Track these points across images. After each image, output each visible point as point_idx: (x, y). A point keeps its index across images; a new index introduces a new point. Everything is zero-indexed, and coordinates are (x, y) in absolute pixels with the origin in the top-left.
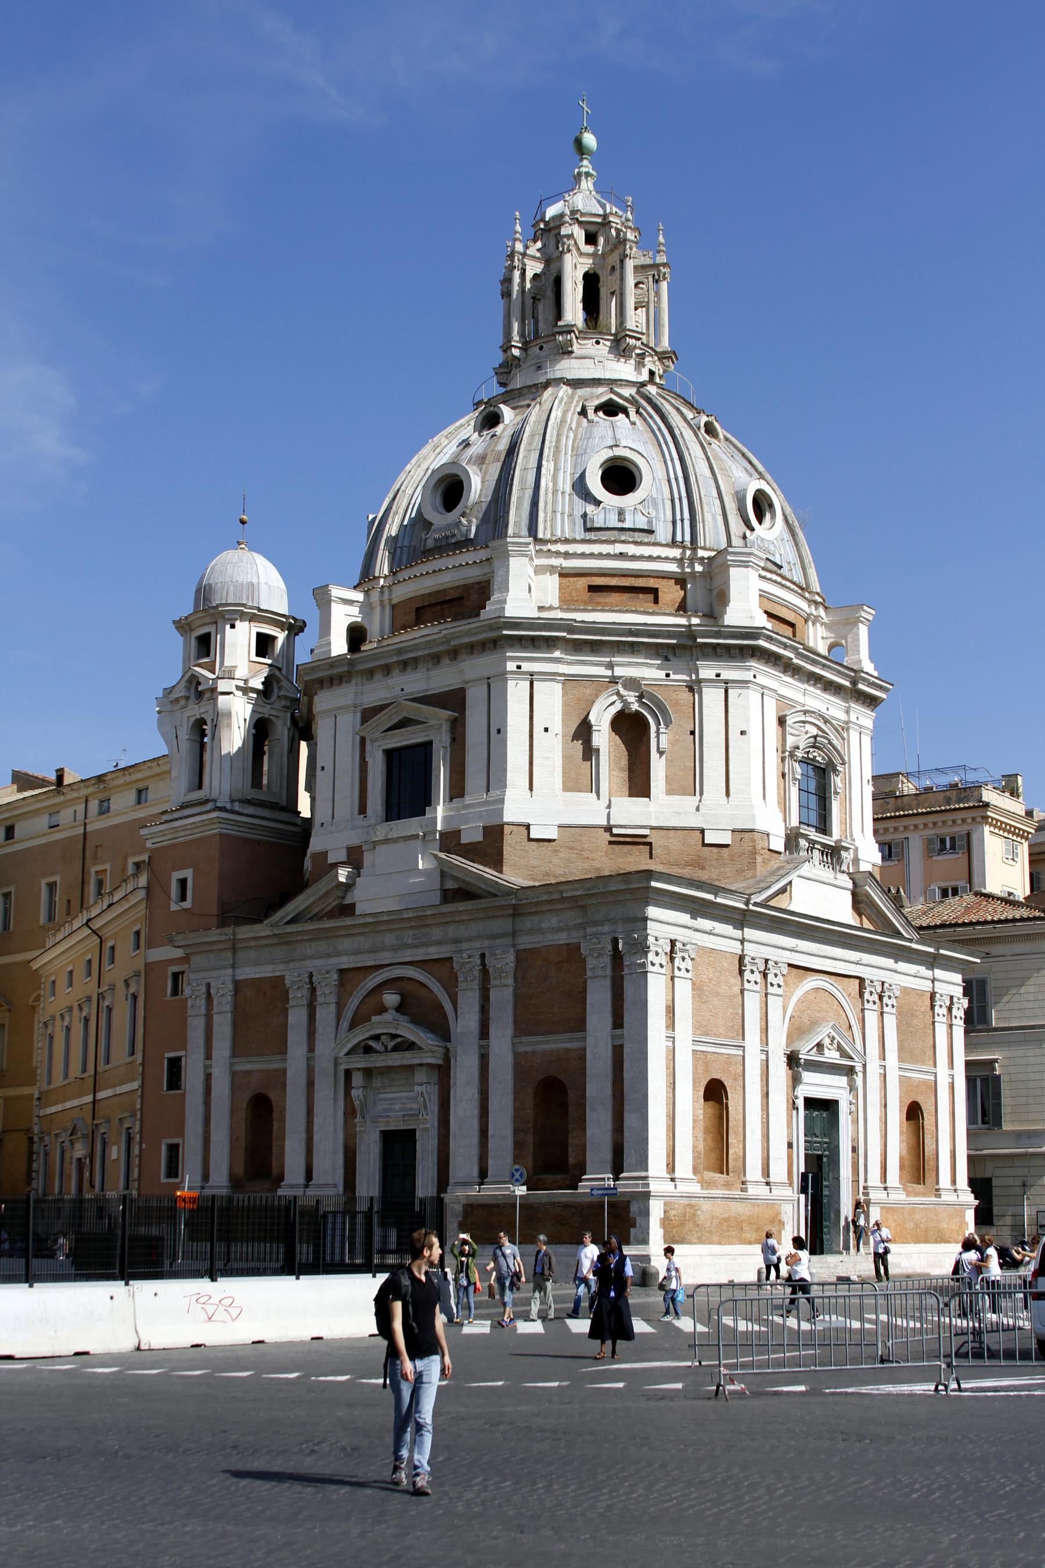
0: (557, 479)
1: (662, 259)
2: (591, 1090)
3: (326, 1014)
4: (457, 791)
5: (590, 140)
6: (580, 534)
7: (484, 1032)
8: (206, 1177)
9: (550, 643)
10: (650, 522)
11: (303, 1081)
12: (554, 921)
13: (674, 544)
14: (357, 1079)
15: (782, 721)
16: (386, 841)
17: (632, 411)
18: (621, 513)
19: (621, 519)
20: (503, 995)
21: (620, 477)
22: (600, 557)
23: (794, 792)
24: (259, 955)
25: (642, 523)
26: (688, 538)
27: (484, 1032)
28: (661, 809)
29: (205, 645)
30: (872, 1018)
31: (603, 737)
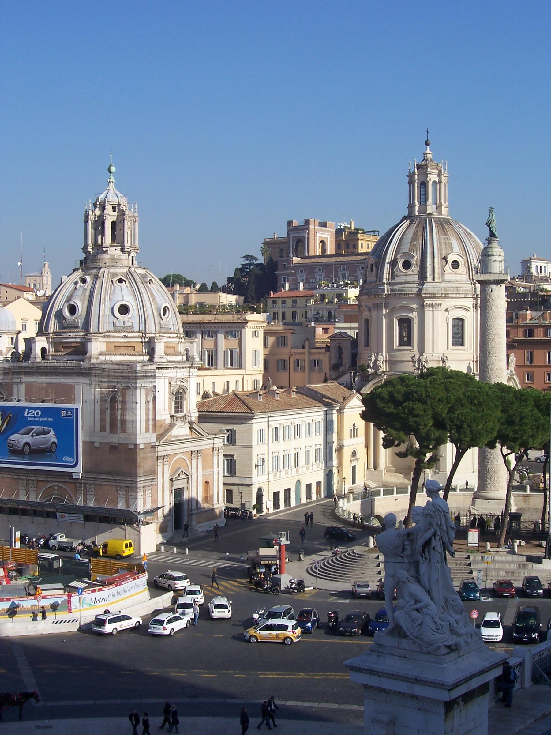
0: (105, 311)
1: (136, 214)
5: (113, 169)
6: (112, 329)
10: (132, 324)
13: (139, 332)
15: (170, 383)
17: (127, 281)
18: (124, 322)
19: (124, 324)
21: (124, 310)
22: (118, 338)
23: (173, 403)
25: (130, 325)
26: (144, 329)
30: (194, 462)
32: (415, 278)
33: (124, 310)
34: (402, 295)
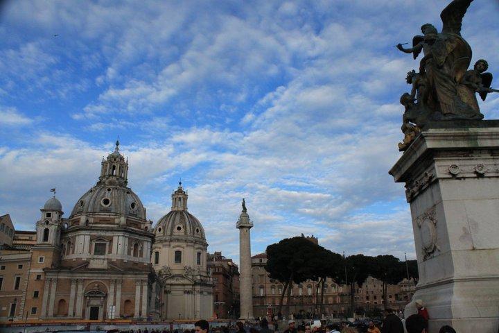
2: (136, 302)
3: (80, 287)
4: (110, 252)
7: (115, 292)
8: (47, 314)
9: (128, 232)
11: (73, 298)
12: (129, 276)
14: (88, 298)
16: (97, 259)
20: (119, 286)
24: (62, 276)
27: (115, 292)
28: (137, 260)
29: (49, 215)
31: (132, 247)
32: (183, 234)
33: (133, 205)
34: (178, 240)
